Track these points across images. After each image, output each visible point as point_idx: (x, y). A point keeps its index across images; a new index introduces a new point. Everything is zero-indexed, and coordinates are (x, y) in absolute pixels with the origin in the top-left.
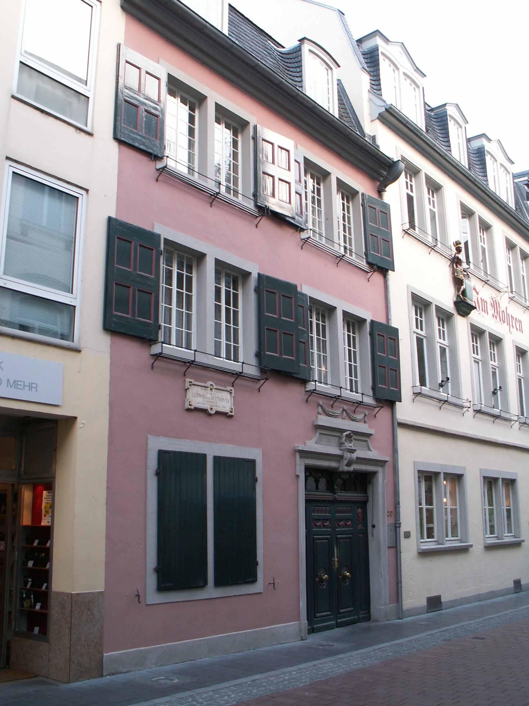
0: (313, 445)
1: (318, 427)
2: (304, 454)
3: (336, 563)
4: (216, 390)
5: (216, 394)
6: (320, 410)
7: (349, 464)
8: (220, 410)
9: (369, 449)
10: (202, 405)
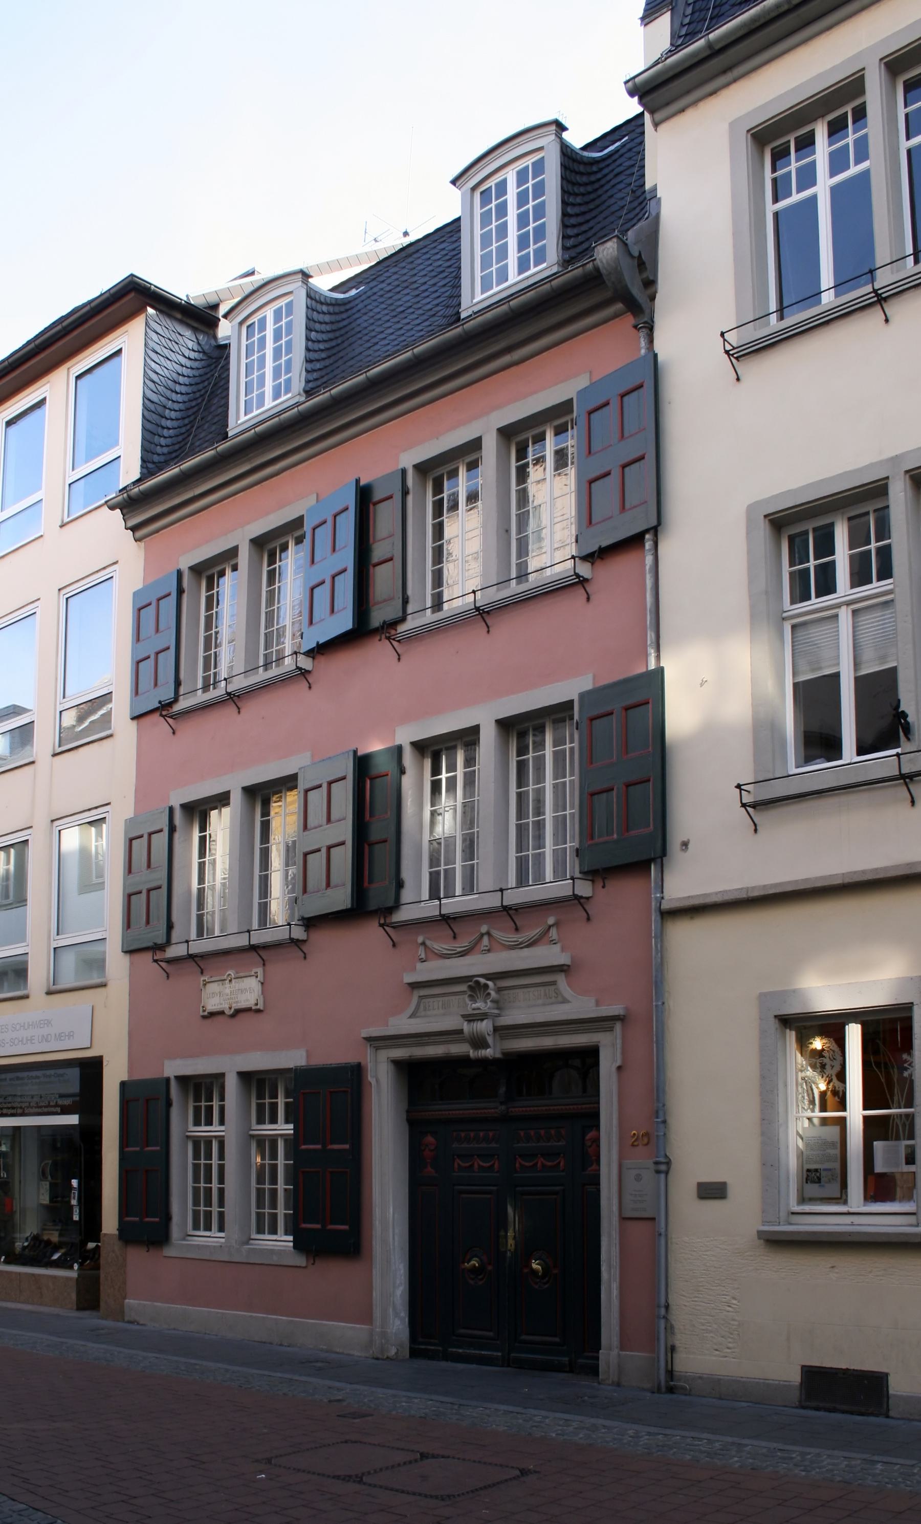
0: (402, 1024)
1: (414, 986)
2: (377, 1042)
3: (511, 1242)
4: (236, 980)
5: (237, 985)
6: (422, 953)
7: (479, 1042)
8: (243, 1007)
9: (565, 1001)
10: (219, 1007)
